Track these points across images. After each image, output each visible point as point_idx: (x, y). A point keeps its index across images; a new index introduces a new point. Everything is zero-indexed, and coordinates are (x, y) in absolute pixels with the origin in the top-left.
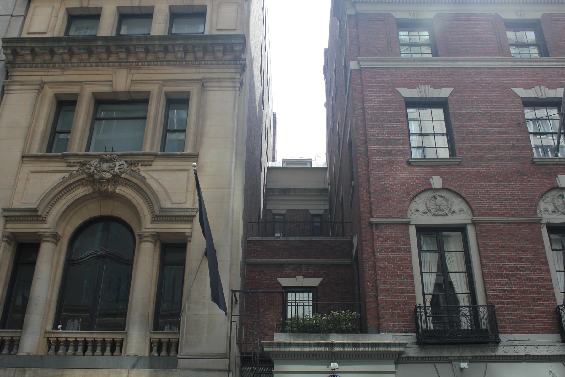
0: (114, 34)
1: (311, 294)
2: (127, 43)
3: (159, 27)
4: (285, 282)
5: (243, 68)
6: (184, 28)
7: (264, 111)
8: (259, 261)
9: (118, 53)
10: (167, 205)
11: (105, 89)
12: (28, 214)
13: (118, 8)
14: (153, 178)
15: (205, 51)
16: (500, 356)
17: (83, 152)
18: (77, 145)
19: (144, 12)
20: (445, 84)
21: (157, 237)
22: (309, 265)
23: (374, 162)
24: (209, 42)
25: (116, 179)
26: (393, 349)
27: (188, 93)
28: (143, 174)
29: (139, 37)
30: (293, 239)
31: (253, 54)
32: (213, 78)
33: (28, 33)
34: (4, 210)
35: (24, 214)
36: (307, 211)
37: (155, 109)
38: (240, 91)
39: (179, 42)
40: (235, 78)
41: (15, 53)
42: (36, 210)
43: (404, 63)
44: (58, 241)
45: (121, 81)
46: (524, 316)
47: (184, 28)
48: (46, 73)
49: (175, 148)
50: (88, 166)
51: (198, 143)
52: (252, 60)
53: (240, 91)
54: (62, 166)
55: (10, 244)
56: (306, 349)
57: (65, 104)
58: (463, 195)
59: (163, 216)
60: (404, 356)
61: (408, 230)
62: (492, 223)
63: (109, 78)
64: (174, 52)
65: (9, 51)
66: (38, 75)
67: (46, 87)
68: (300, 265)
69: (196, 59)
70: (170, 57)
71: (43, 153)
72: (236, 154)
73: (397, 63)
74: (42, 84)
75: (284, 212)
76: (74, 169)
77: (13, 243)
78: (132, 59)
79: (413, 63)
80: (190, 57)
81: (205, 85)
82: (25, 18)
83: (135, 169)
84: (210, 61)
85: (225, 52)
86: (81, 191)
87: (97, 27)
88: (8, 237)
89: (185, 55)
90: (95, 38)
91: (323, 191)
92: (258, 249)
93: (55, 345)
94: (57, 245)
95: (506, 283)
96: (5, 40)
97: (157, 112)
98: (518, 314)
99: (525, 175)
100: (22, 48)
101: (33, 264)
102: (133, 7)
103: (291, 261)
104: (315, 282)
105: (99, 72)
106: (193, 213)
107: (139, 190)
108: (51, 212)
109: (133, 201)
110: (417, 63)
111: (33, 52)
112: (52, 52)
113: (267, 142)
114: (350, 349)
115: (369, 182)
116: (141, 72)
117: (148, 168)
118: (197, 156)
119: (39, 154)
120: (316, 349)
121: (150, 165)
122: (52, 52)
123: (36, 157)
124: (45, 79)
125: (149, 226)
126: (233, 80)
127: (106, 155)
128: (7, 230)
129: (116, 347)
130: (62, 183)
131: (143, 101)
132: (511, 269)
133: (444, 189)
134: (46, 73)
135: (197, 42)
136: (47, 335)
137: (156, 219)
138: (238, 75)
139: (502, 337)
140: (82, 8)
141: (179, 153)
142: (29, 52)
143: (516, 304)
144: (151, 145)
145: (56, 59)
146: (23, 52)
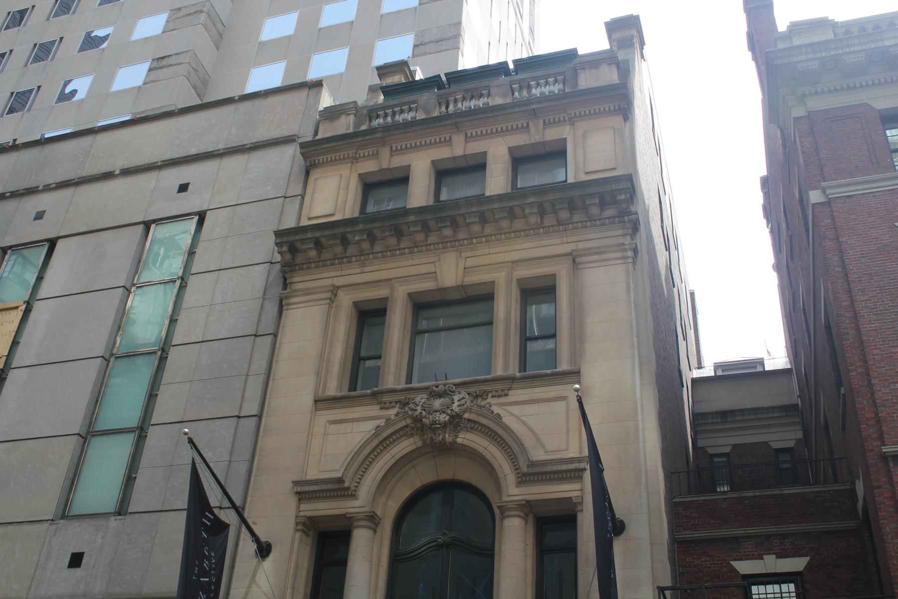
0: (431, 203)
1: (792, 586)
2: (452, 213)
3: (496, 182)
4: (744, 567)
5: (635, 227)
6: (533, 178)
7: (675, 290)
8: (697, 535)
9: (440, 229)
10: (538, 455)
12: (330, 486)
13: (433, 162)
14: (512, 414)
15: (572, 208)
17: (403, 385)
18: (392, 375)
19: (472, 162)
21: (528, 508)
22: (784, 536)
23: (875, 352)
24: (576, 193)
25: (456, 422)
27: (554, 276)
28: (496, 410)
29: (469, 201)
30: (750, 494)
31: (647, 202)
32: (589, 249)
33: (310, 219)
34: (296, 483)
35: (324, 487)
36: (766, 444)
37: (505, 307)
38: (634, 263)
39: (530, 200)
40: (623, 244)
41: (293, 250)
42: (340, 480)
44: (377, 525)
45: (449, 270)
47: (533, 178)
48: (339, 273)
49: (543, 362)
50: (412, 406)
51: (577, 353)
52: (647, 212)
53: (634, 263)
54: (373, 410)
55: (308, 535)
57: (370, 316)
59: (535, 473)
63: (429, 268)
64: (525, 216)
65: (285, 249)
66: (327, 278)
67: (341, 293)
68: (768, 537)
69: (559, 223)
70: (519, 224)
71: (345, 392)
72: (640, 364)
73: (891, 183)
74: (335, 290)
75: (727, 450)
76: (392, 412)
77: (311, 533)
78: (461, 235)
80: (549, 220)
81: (577, 260)
82: (303, 197)
83: (483, 403)
84: (581, 222)
85: (602, 205)
86: (405, 446)
87: (405, 195)
88: (304, 524)
89: (542, 218)
90: (405, 212)
91: (788, 409)
92: (693, 515)
94: (375, 532)
96: (279, 234)
97: (508, 312)
100: (303, 241)
101: (343, 563)
102: (454, 158)
103: (751, 530)
104: (797, 564)
105: (414, 262)
106: (582, 466)
107: (492, 436)
108: (363, 482)
109: (485, 453)
111: (318, 244)
112: (345, 242)
113: (685, 338)
115: (870, 386)
116: (478, 253)
117: (504, 400)
118: (578, 373)
119: (339, 394)
121: (506, 395)
122: (345, 242)
124: (339, 282)
125: (513, 492)
126: (621, 247)
127: (437, 387)
128: (302, 514)
130: (375, 435)
131: (483, 297)
134: (339, 273)
135: (558, 195)
137: (524, 479)
138: (628, 238)
140: (381, 171)
141: (548, 371)
142: (312, 245)
144: (504, 363)
145: (352, 250)
146: (304, 247)
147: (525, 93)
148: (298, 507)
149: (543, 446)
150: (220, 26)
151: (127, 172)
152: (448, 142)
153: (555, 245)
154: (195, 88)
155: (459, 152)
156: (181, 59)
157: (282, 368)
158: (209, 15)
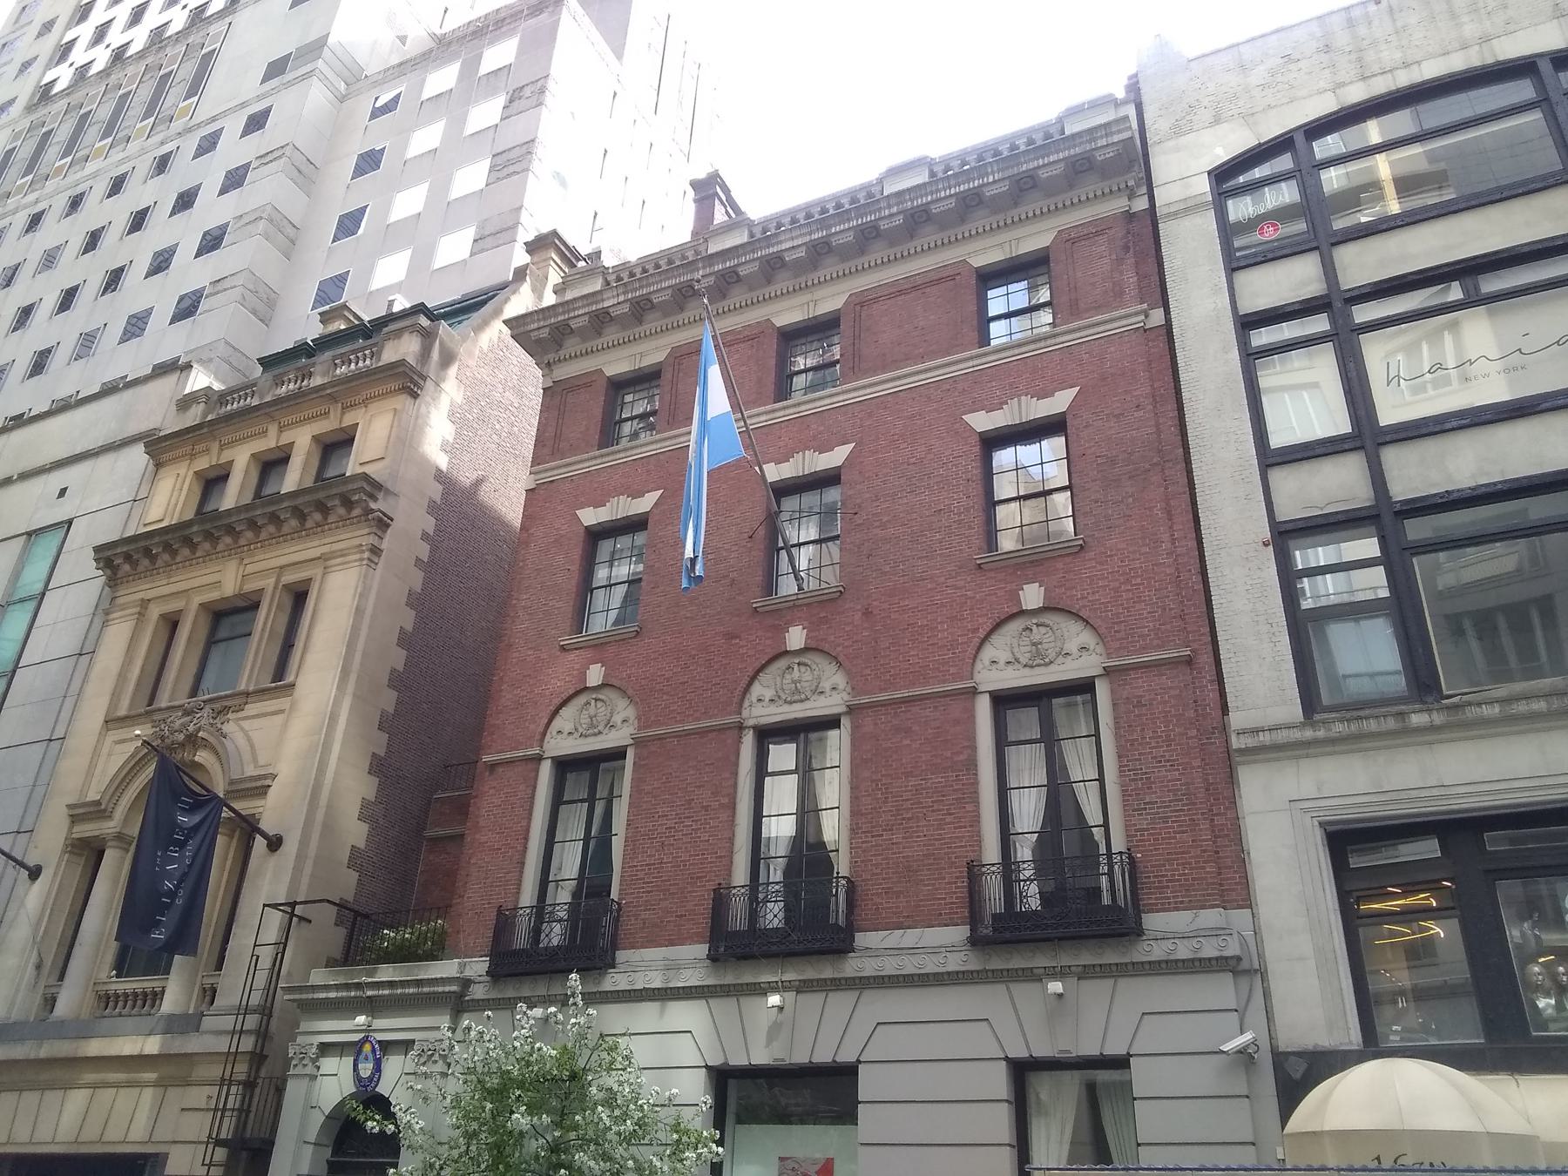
11: (214, 595)
26: (440, 989)
34: (69, 806)
39: (285, 504)
42: (98, 803)
45: (224, 578)
55: (80, 855)
56: (332, 995)
58: (630, 692)
61: (537, 771)
62: (660, 738)
74: (145, 603)
88: (73, 846)
93: (107, 1000)
111: (128, 557)
114: (386, 992)
117: (240, 714)
123: (126, 717)
129: (157, 996)
130: (132, 756)
132: (670, 823)
139: (621, 956)
145: (159, 563)
149: (255, 759)
150: (290, 231)
151: (25, 476)
153: (311, 548)
154: (254, 312)
155: (273, 445)
156: (239, 280)
157: (90, 689)
158: (271, 221)
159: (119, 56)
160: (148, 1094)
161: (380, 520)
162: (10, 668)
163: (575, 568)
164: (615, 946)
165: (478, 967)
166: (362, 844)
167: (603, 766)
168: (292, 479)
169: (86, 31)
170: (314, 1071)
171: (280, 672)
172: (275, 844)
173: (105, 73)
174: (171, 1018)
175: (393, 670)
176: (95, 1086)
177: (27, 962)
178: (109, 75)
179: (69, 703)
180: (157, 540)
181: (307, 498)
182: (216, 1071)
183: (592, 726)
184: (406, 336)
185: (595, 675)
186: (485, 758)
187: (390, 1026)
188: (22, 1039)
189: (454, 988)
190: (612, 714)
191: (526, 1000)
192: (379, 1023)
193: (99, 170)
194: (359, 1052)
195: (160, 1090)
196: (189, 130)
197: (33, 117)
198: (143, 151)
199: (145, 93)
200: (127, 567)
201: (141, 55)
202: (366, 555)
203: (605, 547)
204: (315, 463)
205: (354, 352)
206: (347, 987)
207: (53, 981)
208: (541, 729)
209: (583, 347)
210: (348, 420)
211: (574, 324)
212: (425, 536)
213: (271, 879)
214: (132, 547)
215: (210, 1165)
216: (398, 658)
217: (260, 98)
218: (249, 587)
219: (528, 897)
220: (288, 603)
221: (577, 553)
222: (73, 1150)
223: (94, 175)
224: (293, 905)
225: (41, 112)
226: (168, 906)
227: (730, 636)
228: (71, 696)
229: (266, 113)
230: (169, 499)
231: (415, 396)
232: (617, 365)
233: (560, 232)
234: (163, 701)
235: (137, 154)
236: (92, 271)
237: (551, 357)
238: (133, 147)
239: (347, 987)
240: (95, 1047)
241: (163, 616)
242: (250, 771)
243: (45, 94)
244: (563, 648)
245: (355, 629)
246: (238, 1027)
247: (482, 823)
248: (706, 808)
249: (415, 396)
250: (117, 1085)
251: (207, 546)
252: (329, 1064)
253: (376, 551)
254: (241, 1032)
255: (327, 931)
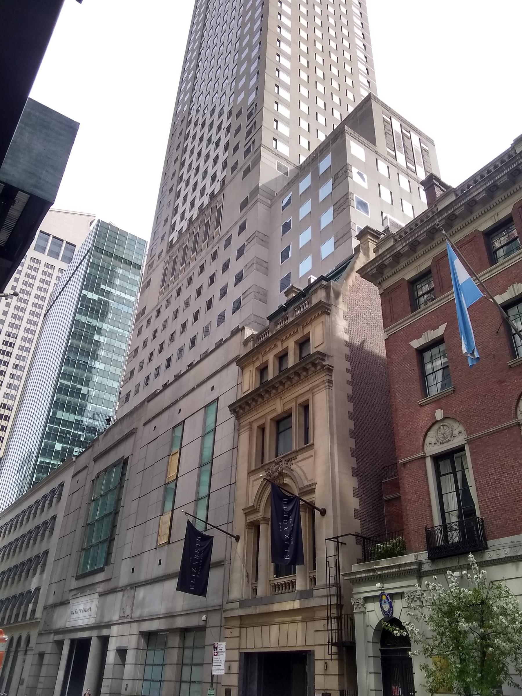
11: (274, 415)
16: (488, 561)
20: (441, 322)
26: (409, 568)
39: (291, 372)
42: (253, 506)
43: (413, 318)
46: (508, 519)
55: (252, 529)
56: (363, 575)
58: (458, 419)
60: (422, 571)
62: (480, 438)
67: (253, 424)
69: (305, 377)
74: (251, 424)
79: (418, 315)
88: (248, 525)
93: (275, 587)
95: (493, 491)
98: (503, 518)
99: (504, 382)
110: (421, 314)
111: (240, 407)
114: (386, 572)
117: (296, 460)
120: (368, 574)
122: (260, 396)
128: (248, 521)
129: (293, 584)
130: (261, 485)
133: (445, 418)
136: (271, 582)
139: (490, 543)
143: (501, 510)
145: (252, 406)
147: (286, 321)
148: (246, 518)
149: (307, 479)
150: (265, 265)
151: (199, 386)
152: (276, 346)
154: (260, 300)
156: (252, 290)
157: (240, 461)
158: (257, 263)
159: (190, 222)
160: (300, 624)
161: (329, 369)
162: (210, 459)
163: (416, 368)
164: (485, 539)
165: (423, 556)
166: (358, 508)
167: (455, 456)
168: (291, 361)
169: (178, 217)
170: (364, 610)
171: (306, 440)
172: (323, 512)
173: (188, 229)
174: (301, 592)
175: (350, 430)
176: (280, 623)
177: (243, 575)
178: (189, 230)
179: (234, 468)
180: (249, 398)
181: (299, 367)
182: (324, 614)
183: (444, 438)
184: (319, 291)
185: (439, 414)
186: (400, 461)
187: (392, 587)
188: (249, 606)
189: (415, 567)
190: (452, 431)
191: (450, 569)
192: (386, 586)
193: (195, 265)
194: (381, 600)
195: (304, 623)
196: (220, 240)
197: (170, 253)
198: (207, 253)
199: (202, 231)
200: (241, 411)
201: (197, 218)
202: (327, 384)
203: (427, 355)
204: (298, 352)
205: (301, 304)
206: (368, 571)
207: (254, 581)
208: (421, 444)
209: (393, 271)
210: (306, 332)
211: (386, 263)
212: (348, 371)
213: (326, 528)
214: (241, 403)
215: (332, 654)
216: (351, 424)
217: (241, 218)
218: (287, 407)
219: (437, 521)
220: (302, 410)
221: (415, 361)
222: (279, 650)
223: (194, 268)
224: (337, 538)
225: (172, 251)
226: (288, 545)
227: (500, 382)
228: (234, 466)
229: (245, 223)
230: (249, 382)
231: (329, 314)
232: (410, 274)
233: (369, 226)
234: (267, 461)
235: (206, 255)
236: (202, 302)
237: (380, 280)
238: (203, 253)
239: (368, 571)
240: (276, 607)
241: (258, 427)
242: (306, 483)
243: (171, 245)
244: (421, 405)
245: (331, 416)
246: (328, 594)
247: (407, 491)
248: (513, 467)
249: (329, 314)
250: (288, 623)
251: (267, 396)
252: (370, 606)
253: (330, 382)
254: (330, 595)
255: (354, 548)
